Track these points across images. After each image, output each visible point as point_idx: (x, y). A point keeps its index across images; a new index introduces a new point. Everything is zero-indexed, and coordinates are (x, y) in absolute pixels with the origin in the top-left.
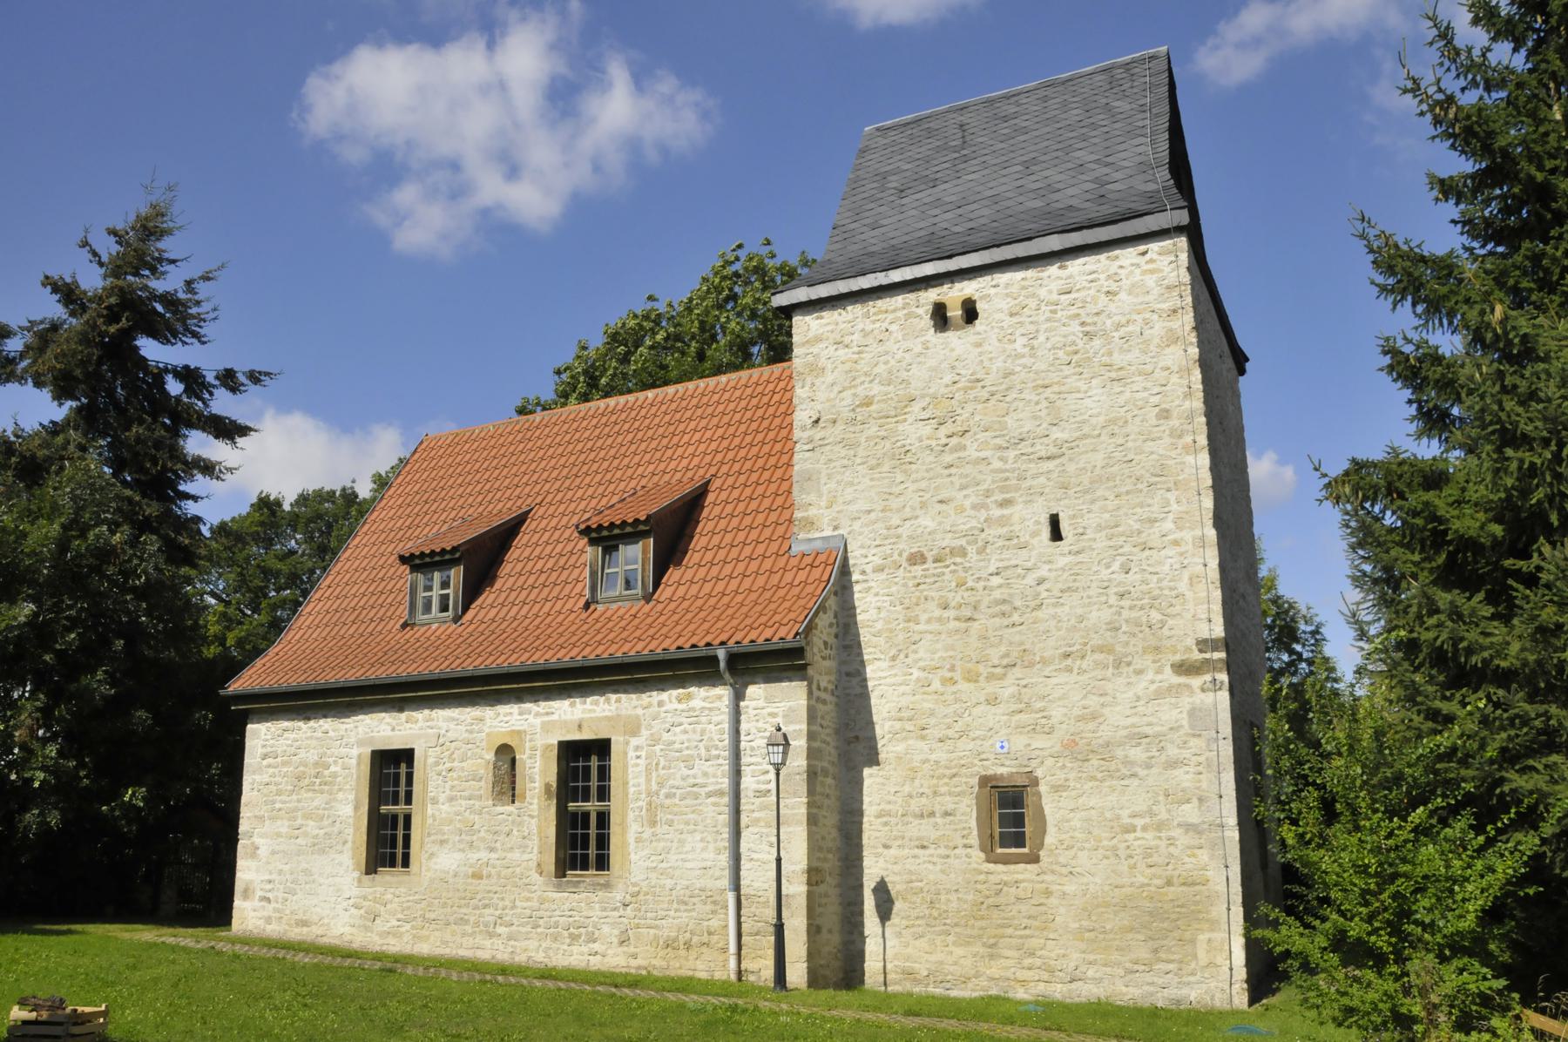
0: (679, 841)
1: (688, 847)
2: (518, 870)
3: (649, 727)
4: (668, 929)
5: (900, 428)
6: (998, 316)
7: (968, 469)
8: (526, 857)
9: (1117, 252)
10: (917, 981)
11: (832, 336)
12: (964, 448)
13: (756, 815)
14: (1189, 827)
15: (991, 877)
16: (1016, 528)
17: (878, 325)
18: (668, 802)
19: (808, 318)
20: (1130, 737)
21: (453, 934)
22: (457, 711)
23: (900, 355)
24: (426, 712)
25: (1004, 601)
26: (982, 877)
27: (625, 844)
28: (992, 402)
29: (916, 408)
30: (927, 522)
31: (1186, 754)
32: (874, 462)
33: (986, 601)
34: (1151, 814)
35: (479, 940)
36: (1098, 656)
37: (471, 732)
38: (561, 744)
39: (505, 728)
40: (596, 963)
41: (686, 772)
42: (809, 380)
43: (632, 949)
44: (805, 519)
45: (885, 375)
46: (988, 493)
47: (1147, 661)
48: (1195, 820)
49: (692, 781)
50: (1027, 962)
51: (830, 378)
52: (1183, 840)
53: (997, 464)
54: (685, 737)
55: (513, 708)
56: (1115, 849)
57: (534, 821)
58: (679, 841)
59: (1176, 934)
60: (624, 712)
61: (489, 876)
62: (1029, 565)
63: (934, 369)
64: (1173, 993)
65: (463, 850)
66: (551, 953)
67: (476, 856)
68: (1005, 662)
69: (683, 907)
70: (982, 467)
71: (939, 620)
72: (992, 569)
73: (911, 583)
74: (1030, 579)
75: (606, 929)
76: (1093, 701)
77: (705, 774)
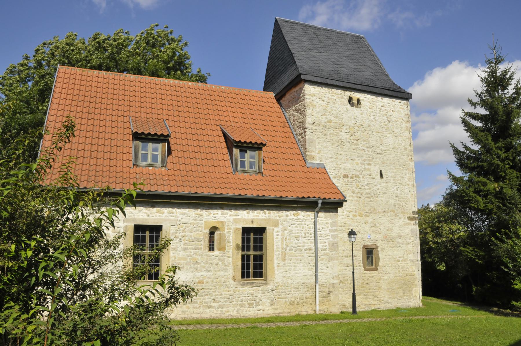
0: (295, 266)
1: (298, 268)
2: (223, 279)
3: (282, 224)
4: (290, 298)
5: (340, 133)
6: (366, 107)
7: (359, 152)
8: (226, 273)
9: (394, 100)
10: (346, 308)
11: (318, 96)
12: (358, 145)
13: (322, 257)
14: (411, 261)
15: (367, 275)
16: (372, 172)
17: (333, 97)
18: (290, 252)
19: (310, 86)
20: (399, 236)
21: (188, 308)
22: (187, 210)
23: (340, 109)
24: (170, 209)
25: (369, 194)
26: (364, 275)
27: (273, 268)
28: (365, 133)
29: (344, 128)
30: (348, 165)
31: (410, 241)
32: (332, 142)
33: (365, 193)
34: (404, 257)
35: (202, 310)
36: (392, 213)
37: (195, 220)
38: (242, 228)
39: (215, 220)
40: (261, 314)
41: (297, 241)
42: (311, 108)
43: (276, 307)
44: (311, 156)
45: (335, 114)
46: (365, 160)
47: (401, 216)
48: (412, 259)
49: (299, 245)
50: (375, 299)
51: (318, 110)
52: (410, 264)
53: (367, 152)
54: (297, 229)
55: (245, 212)
56: (395, 266)
57: (231, 259)
58: (295, 266)
59: (408, 288)
60: (271, 218)
61: (207, 282)
62: (375, 184)
63: (350, 117)
64: (408, 304)
65: (193, 272)
66: (240, 312)
67: (200, 274)
68: (370, 212)
69: (296, 290)
70: (363, 152)
71: (352, 196)
72: (366, 184)
73: (344, 184)
74: (375, 188)
75: (265, 300)
76: (390, 225)
77: (304, 243)
